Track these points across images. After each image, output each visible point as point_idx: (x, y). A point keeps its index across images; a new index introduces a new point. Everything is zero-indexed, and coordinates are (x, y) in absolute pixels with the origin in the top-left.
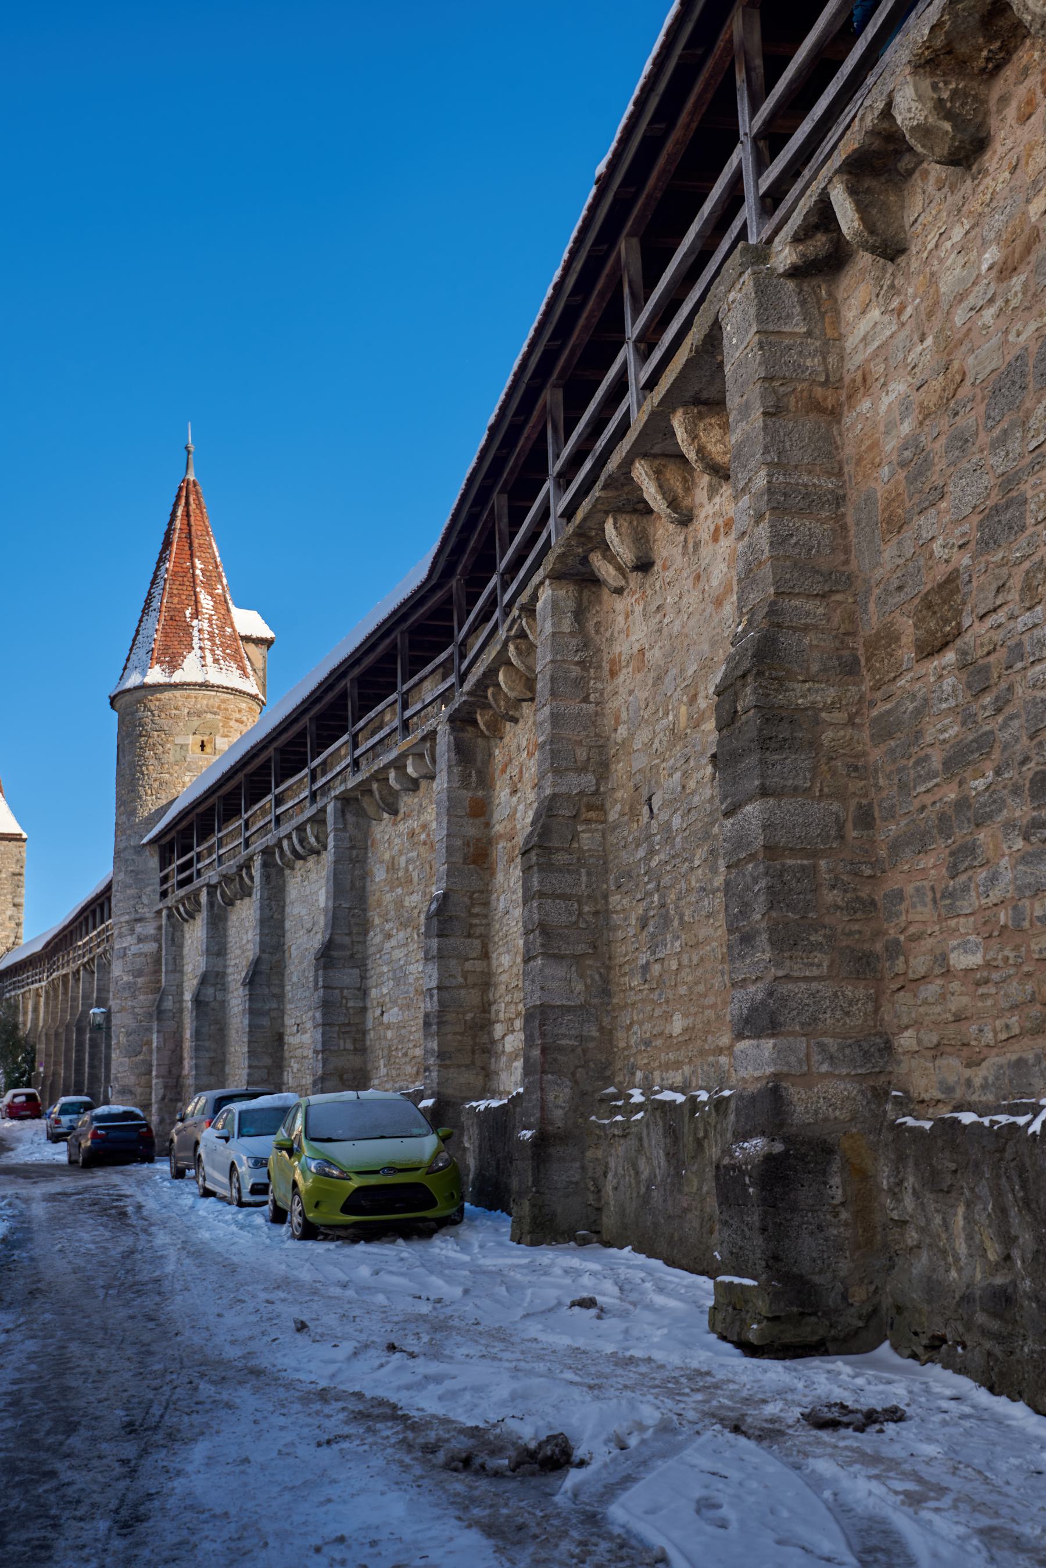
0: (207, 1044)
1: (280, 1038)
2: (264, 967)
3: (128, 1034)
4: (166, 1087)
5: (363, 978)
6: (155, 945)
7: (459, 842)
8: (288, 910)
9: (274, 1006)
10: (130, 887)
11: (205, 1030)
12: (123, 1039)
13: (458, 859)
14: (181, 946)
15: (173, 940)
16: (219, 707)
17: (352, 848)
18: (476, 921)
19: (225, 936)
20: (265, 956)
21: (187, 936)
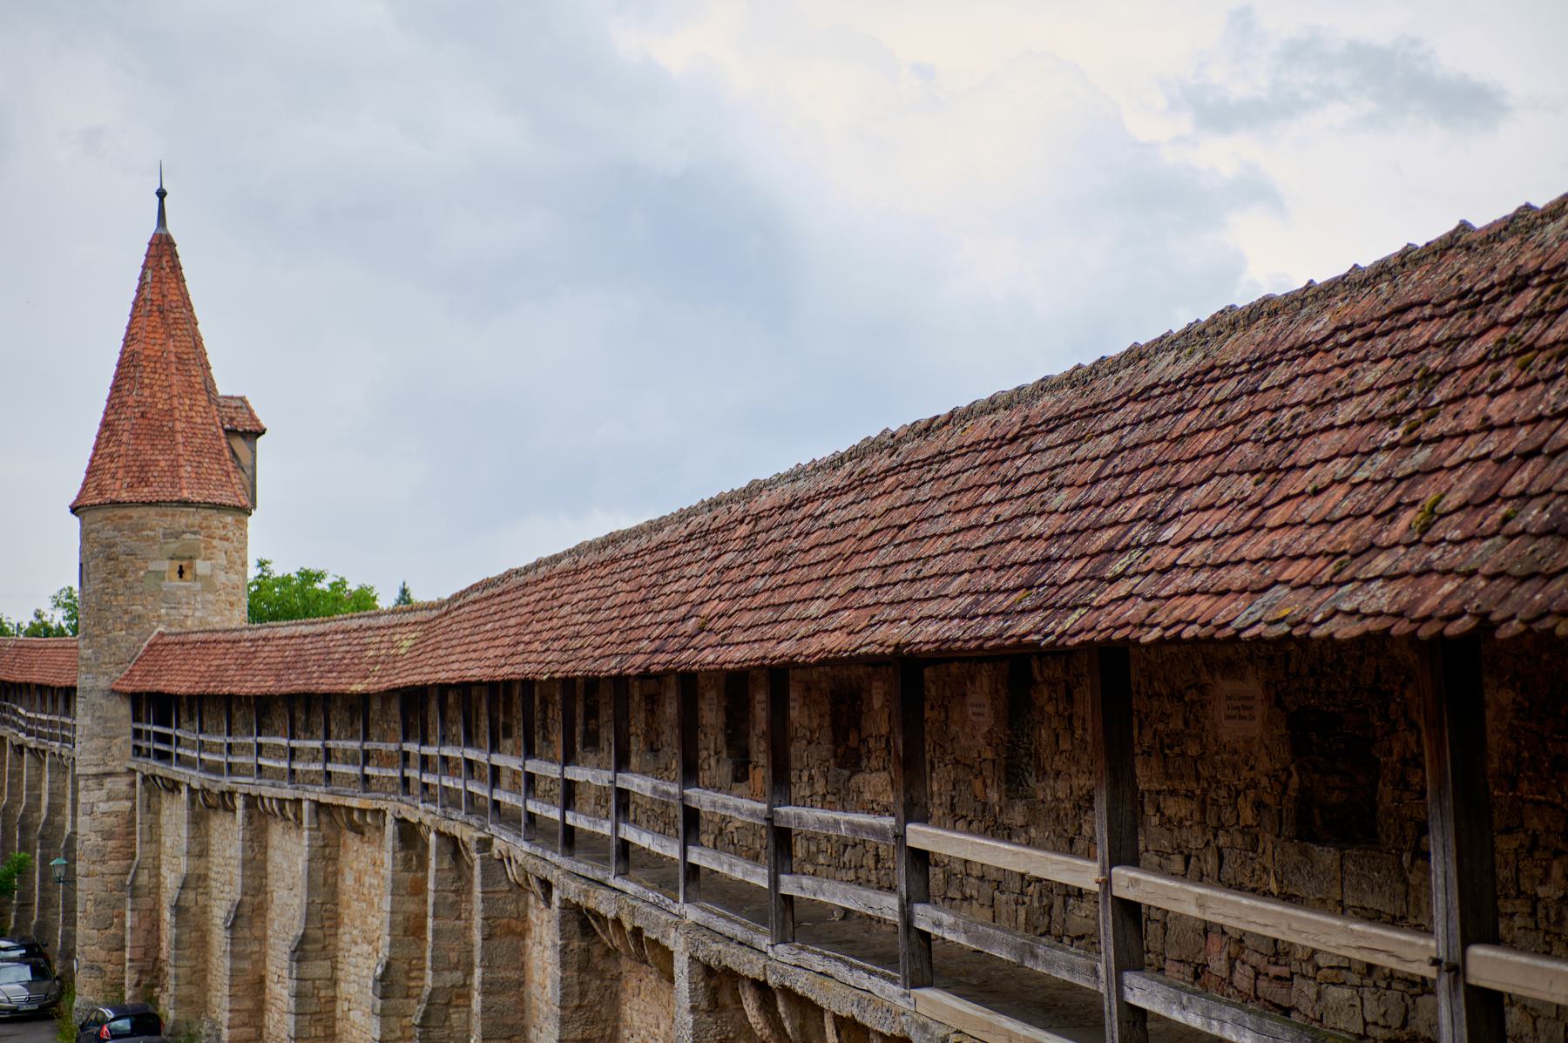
0: (187, 952)
1: (261, 980)
2: (246, 910)
3: (97, 903)
4: (141, 972)
5: (334, 968)
6: (129, 804)
7: (400, 918)
8: (271, 852)
9: (256, 949)
10: (98, 736)
11: (185, 937)
12: (90, 907)
13: (399, 931)
14: (158, 813)
15: (149, 806)
16: (200, 526)
17: (325, 846)
18: (413, 984)
19: (207, 835)
20: (248, 899)
21: (165, 804)
